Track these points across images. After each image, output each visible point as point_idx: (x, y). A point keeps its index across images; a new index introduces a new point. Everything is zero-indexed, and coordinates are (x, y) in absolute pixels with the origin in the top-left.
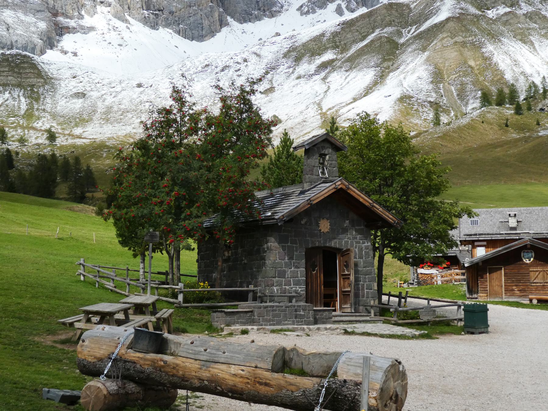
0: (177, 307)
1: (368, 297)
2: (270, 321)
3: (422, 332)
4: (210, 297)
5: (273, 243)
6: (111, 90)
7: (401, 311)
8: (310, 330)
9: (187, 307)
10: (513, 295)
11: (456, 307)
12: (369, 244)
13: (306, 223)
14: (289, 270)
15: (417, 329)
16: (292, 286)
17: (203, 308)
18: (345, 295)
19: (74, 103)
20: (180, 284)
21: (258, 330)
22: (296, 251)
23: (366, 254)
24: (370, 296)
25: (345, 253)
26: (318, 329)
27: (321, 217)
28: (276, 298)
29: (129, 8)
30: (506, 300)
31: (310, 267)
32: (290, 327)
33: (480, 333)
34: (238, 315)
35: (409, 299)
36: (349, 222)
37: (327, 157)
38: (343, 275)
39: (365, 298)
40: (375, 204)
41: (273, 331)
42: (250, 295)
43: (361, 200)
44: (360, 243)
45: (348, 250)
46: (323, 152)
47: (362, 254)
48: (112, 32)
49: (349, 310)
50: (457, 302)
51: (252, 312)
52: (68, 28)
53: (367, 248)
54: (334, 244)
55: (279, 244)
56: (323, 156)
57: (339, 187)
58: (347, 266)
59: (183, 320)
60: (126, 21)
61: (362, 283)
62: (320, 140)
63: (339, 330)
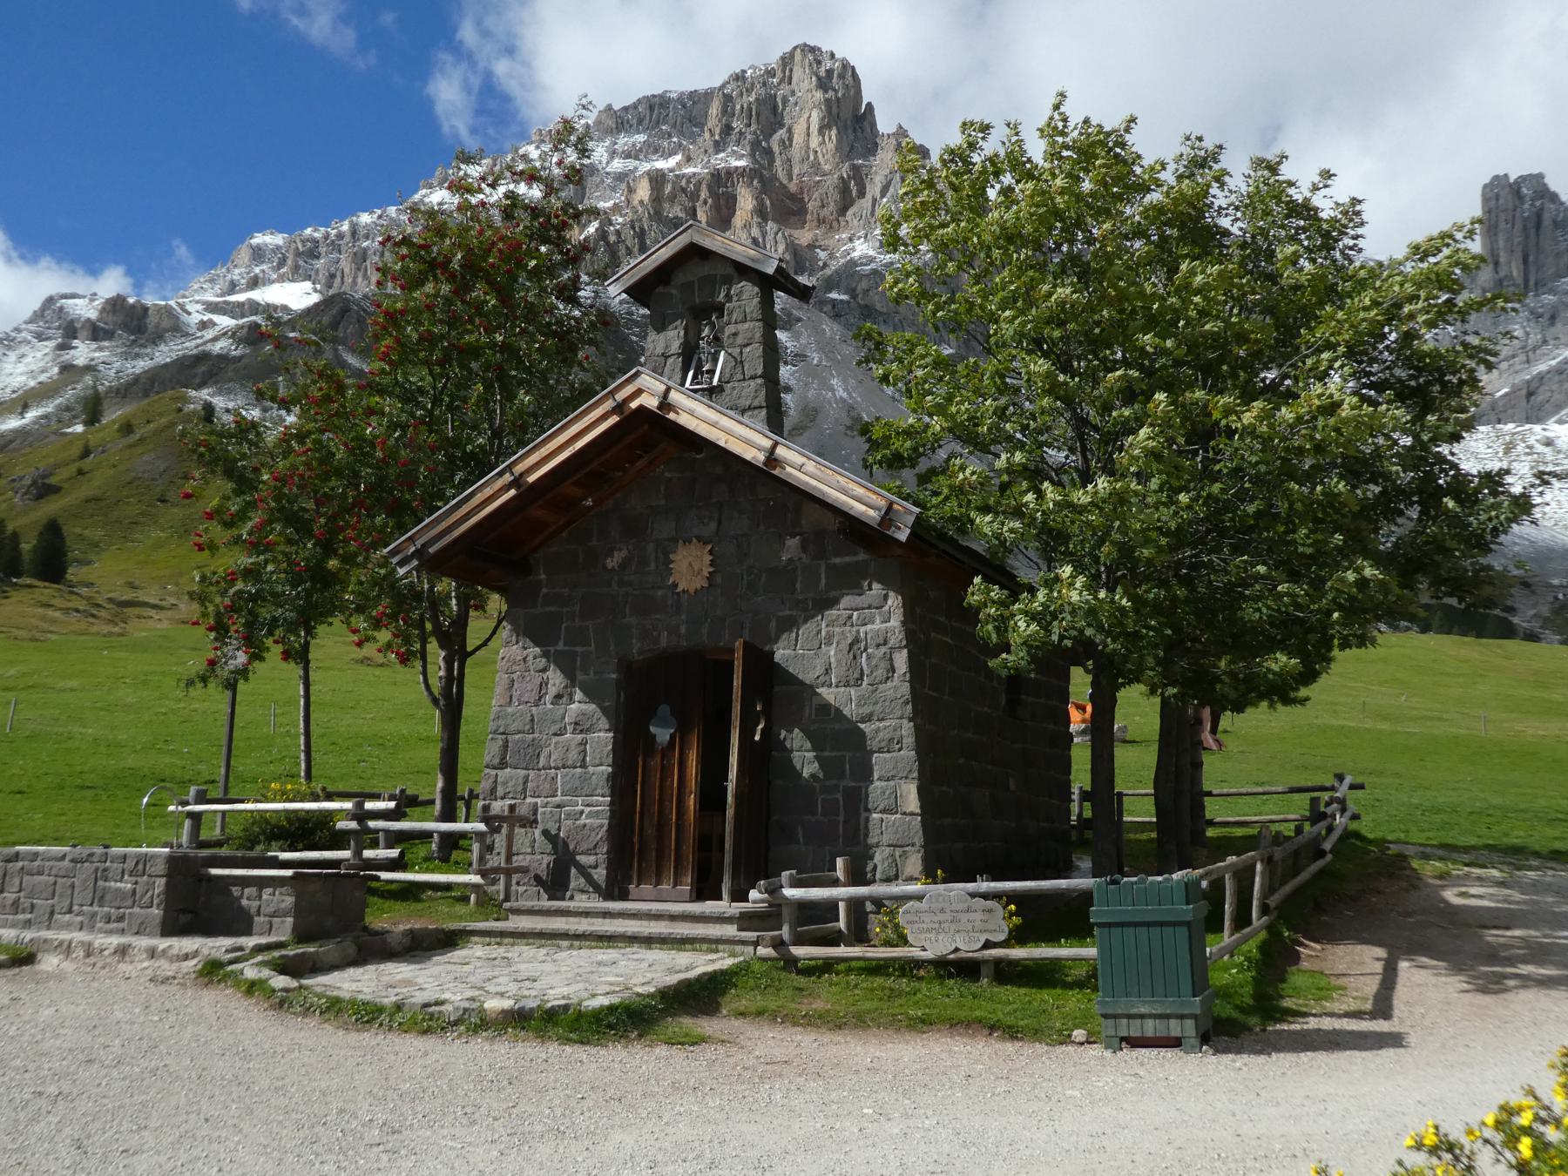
13: (624, 565)
14: (555, 739)
16: (558, 799)
27: (682, 537)
57: (634, 405)
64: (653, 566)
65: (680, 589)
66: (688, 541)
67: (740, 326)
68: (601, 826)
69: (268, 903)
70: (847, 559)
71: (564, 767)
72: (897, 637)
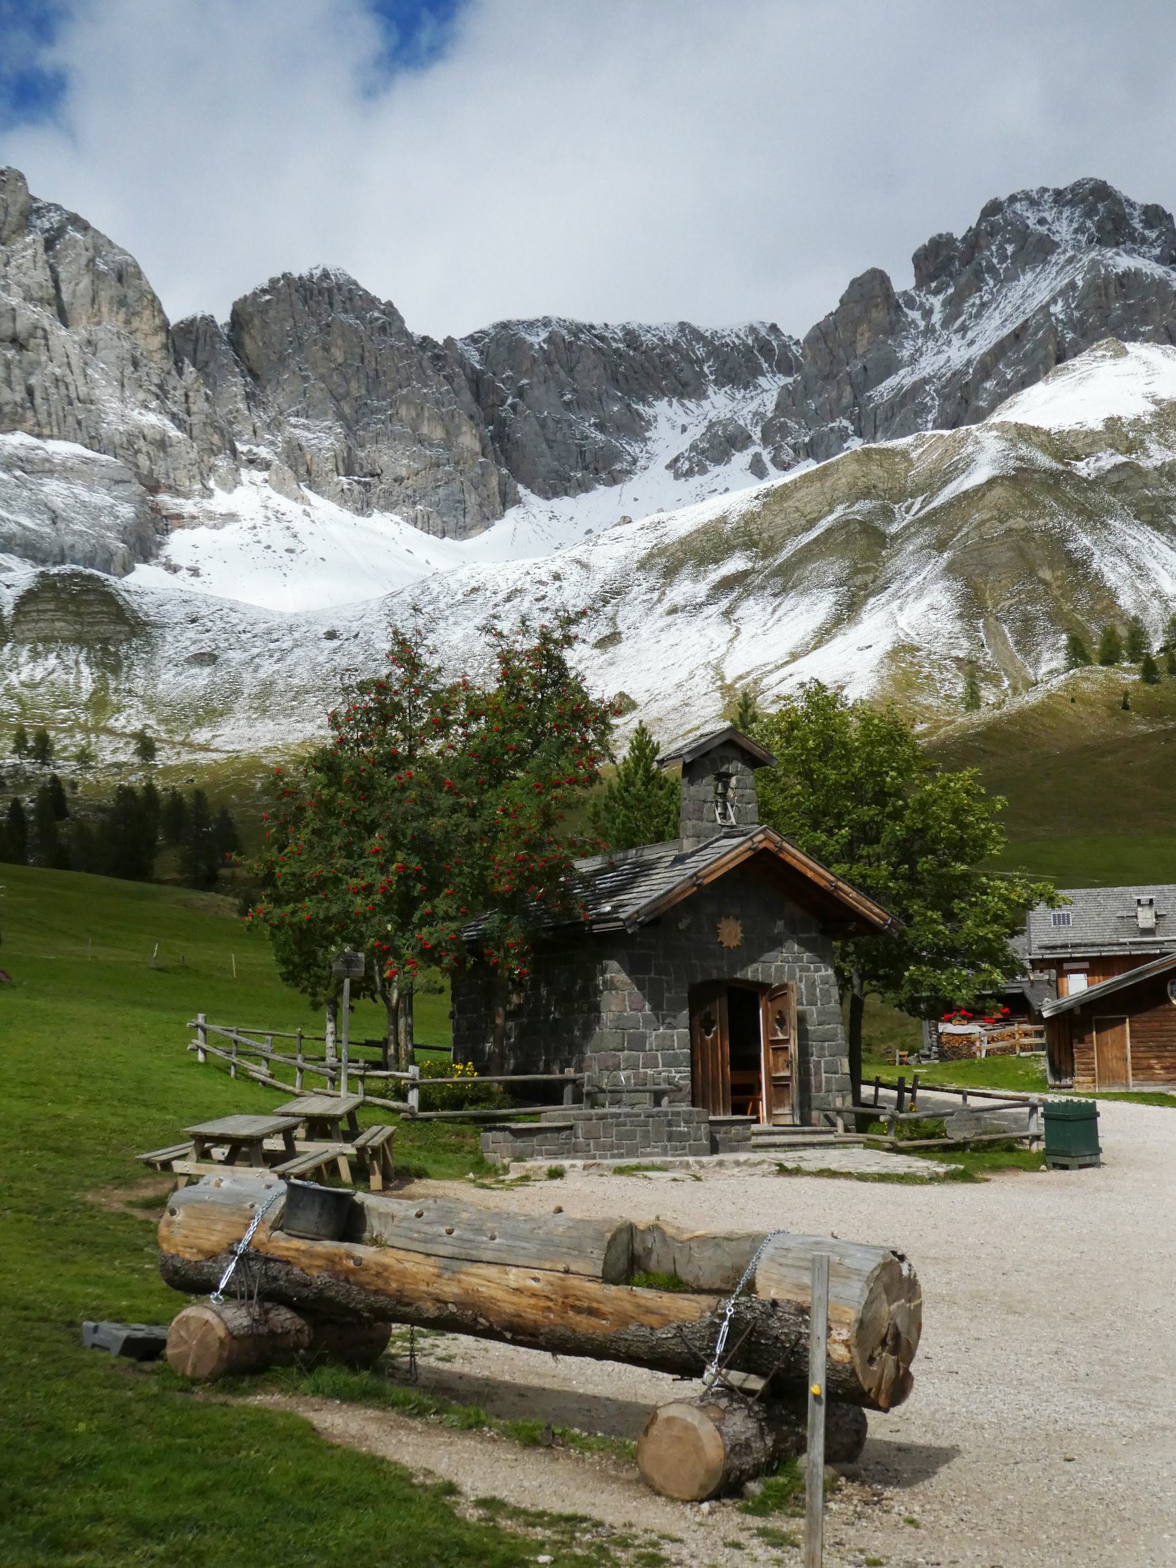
0: (406, 1119)
2: (612, 1147)
3: (953, 1166)
4: (480, 1096)
5: (615, 972)
6: (272, 646)
7: (904, 1120)
8: (702, 1166)
9: (428, 1120)
10: (1152, 1078)
11: (1027, 1110)
12: (830, 972)
15: (942, 1161)
17: (464, 1121)
18: (779, 1085)
19: (192, 676)
20: (411, 1068)
21: (585, 1168)
23: (823, 995)
25: (778, 993)
26: (721, 1164)
28: (625, 1096)
29: (308, 472)
30: (1135, 1090)
31: (700, 1025)
32: (658, 1160)
33: (1081, 1167)
34: (540, 1137)
35: (920, 1093)
36: (786, 925)
37: (733, 781)
38: (773, 1042)
39: (822, 1094)
40: (840, 884)
41: (619, 1171)
42: (568, 1091)
43: (810, 874)
44: (808, 970)
45: (784, 986)
46: (723, 770)
47: (814, 995)
48: (273, 522)
49: (788, 1120)
50: (1027, 1099)
51: (571, 1128)
52: (179, 517)
53: (825, 981)
54: (751, 973)
56: (724, 778)
57: (761, 846)
58: (782, 1022)
59: (419, 1148)
60: (304, 500)
61: (814, 1058)
62: (718, 742)
63: (765, 1166)
72: (833, 979)
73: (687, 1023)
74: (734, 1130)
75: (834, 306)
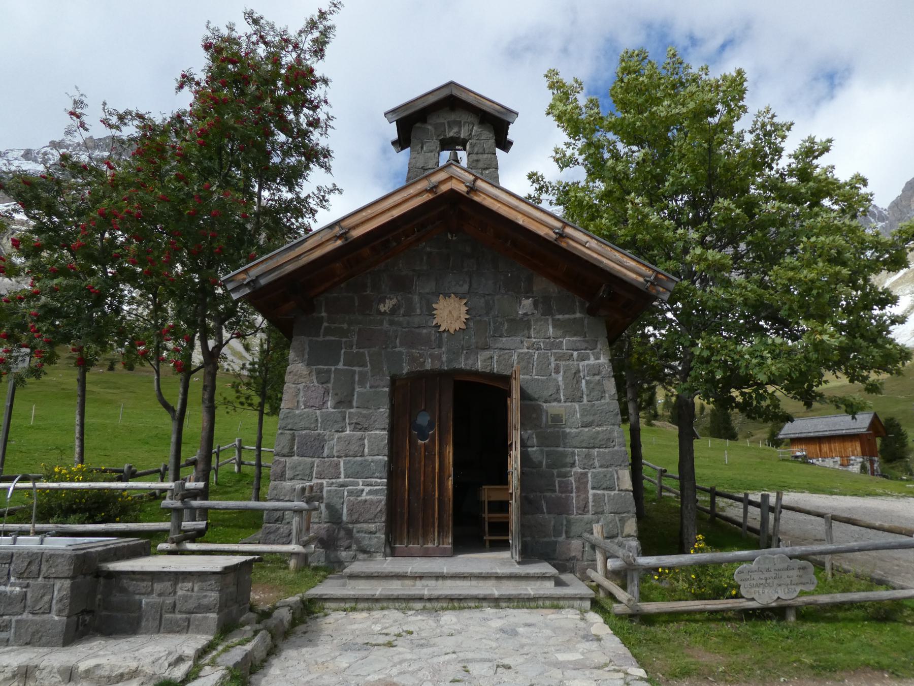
1: (602, 513)
12: (604, 360)
13: (394, 311)
14: (337, 435)
16: (342, 480)
22: (362, 383)
23: (591, 390)
24: (607, 508)
43: (521, 220)
46: (451, 134)
47: (578, 388)
54: (480, 363)
55: (308, 365)
57: (444, 188)
64: (418, 311)
65: (442, 329)
66: (447, 295)
67: (480, 156)
68: (380, 501)
69: (185, 598)
70: (567, 316)
71: (346, 456)
72: (607, 369)
73: (385, 422)
74: (183, 589)
75: (900, 193)
